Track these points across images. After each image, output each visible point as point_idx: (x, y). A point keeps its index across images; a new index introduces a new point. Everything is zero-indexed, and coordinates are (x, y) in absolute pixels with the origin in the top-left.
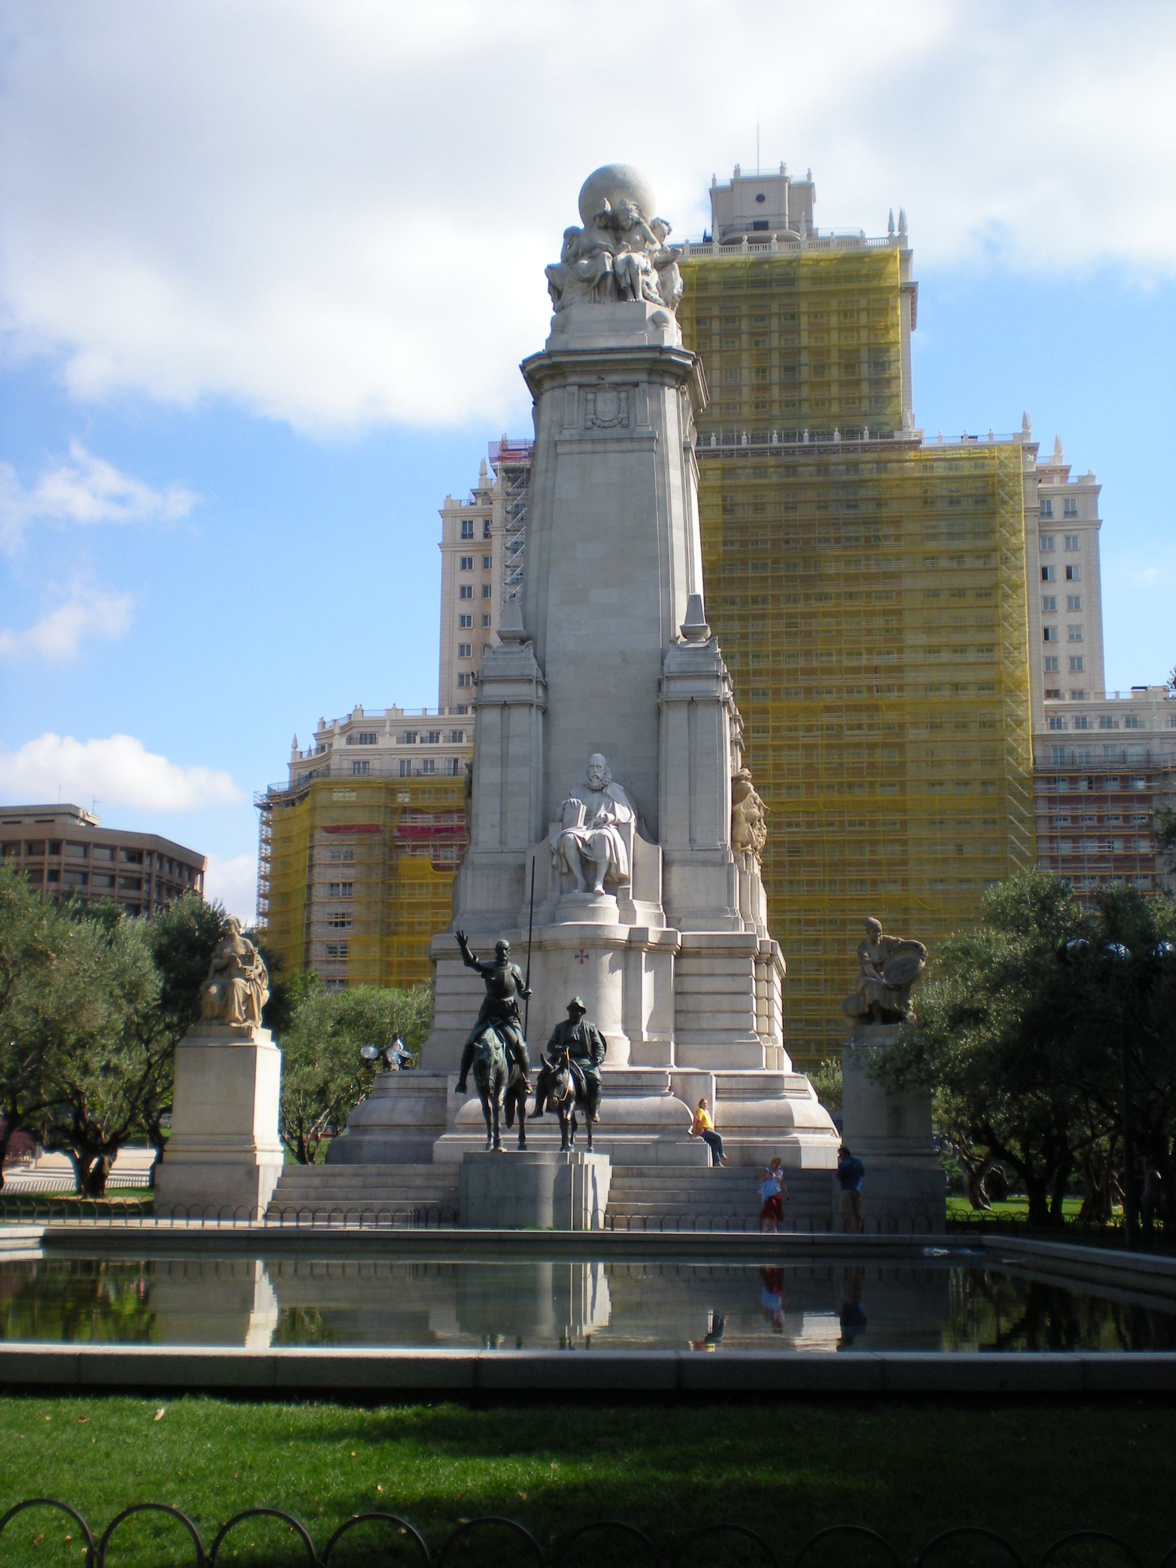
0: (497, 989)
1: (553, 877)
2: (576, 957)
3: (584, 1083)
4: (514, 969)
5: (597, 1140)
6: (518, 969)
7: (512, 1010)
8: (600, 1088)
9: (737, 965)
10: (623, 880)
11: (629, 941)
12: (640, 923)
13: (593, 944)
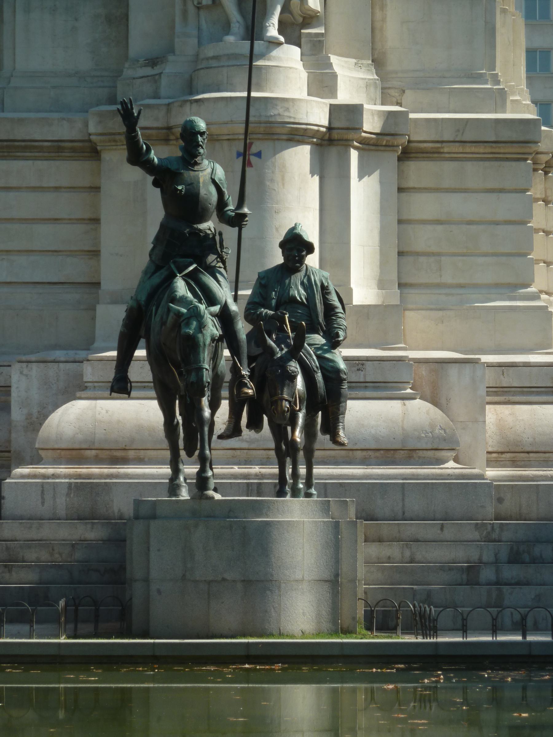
0: (184, 207)
1: (185, 13)
2: (239, 155)
3: (319, 376)
4: (211, 172)
5: (321, 477)
6: (220, 173)
7: (210, 245)
8: (345, 386)
9: (511, 174)
10: (310, 19)
11: (330, 128)
12: (345, 96)
13: (260, 134)
